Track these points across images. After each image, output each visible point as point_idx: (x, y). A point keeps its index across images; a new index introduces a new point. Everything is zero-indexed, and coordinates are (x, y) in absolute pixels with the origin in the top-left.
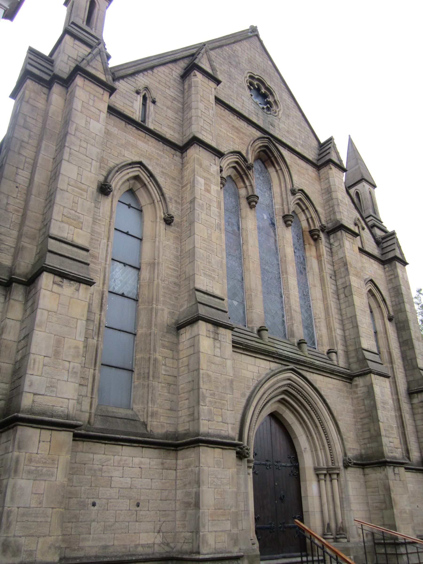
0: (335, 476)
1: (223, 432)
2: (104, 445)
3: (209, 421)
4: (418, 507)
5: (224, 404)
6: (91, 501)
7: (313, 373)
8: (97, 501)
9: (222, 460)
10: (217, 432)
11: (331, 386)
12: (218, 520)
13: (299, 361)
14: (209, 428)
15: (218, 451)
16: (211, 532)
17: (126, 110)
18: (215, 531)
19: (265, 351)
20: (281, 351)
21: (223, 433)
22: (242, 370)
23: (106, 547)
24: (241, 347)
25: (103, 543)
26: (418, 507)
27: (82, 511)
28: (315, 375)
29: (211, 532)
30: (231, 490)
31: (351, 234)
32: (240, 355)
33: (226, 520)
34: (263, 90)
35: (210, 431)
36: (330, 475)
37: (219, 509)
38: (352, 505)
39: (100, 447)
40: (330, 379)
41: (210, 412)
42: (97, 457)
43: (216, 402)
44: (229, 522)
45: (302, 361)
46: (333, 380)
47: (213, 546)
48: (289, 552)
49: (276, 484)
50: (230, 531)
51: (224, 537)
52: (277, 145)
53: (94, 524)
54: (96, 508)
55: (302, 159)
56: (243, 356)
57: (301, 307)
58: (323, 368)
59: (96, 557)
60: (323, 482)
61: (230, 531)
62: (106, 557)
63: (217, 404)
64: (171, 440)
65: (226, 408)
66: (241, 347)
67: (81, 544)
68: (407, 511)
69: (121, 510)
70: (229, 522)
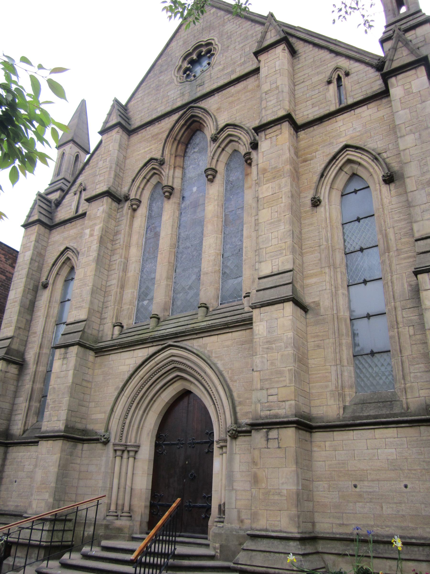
0: (132, 454)
1: (56, 428)
2: (352, 432)
3: (48, 421)
4: (406, 486)
5: (60, 407)
6: (15, 479)
7: (202, 337)
8: (17, 480)
9: (51, 449)
10: (52, 429)
11: (229, 343)
12: (41, 492)
13: (176, 334)
14: (47, 427)
15: (50, 442)
16: (35, 499)
17: (66, 216)
18: (38, 500)
19: (137, 341)
20: (193, 326)
21: (56, 428)
22: (120, 367)
23: (17, 506)
24: (116, 347)
25: (16, 504)
26: (406, 486)
27: (10, 486)
28: (204, 339)
29: (35, 499)
30: (53, 470)
31: (275, 125)
32: (119, 354)
33: (47, 492)
34: (194, 57)
35: (48, 429)
36: (128, 451)
37: (43, 484)
38: (235, 484)
39: (22, 448)
40: (230, 334)
41: (50, 414)
42: (21, 454)
43: (55, 407)
44: (48, 493)
45: (179, 332)
46: (234, 333)
47: (35, 509)
48: (194, 532)
49: (187, 462)
50: (47, 500)
51: (43, 504)
52: (195, 105)
53: (14, 493)
54: (16, 483)
55: (239, 82)
56: (122, 353)
57: (168, 278)
58: (210, 327)
59: (13, 511)
60: (118, 459)
61: (47, 500)
62: (16, 512)
63: (56, 408)
64: (401, 417)
65: (61, 409)
66: (116, 347)
67: (8, 503)
68: (285, 492)
69: (26, 485)
70: (48, 493)
